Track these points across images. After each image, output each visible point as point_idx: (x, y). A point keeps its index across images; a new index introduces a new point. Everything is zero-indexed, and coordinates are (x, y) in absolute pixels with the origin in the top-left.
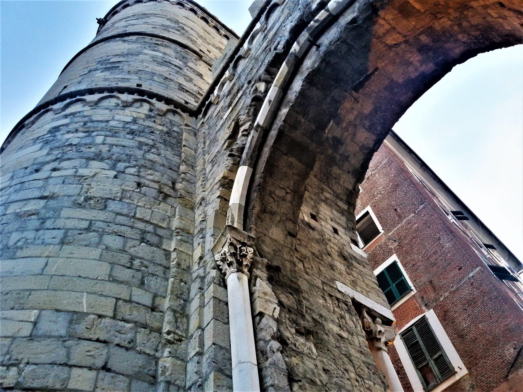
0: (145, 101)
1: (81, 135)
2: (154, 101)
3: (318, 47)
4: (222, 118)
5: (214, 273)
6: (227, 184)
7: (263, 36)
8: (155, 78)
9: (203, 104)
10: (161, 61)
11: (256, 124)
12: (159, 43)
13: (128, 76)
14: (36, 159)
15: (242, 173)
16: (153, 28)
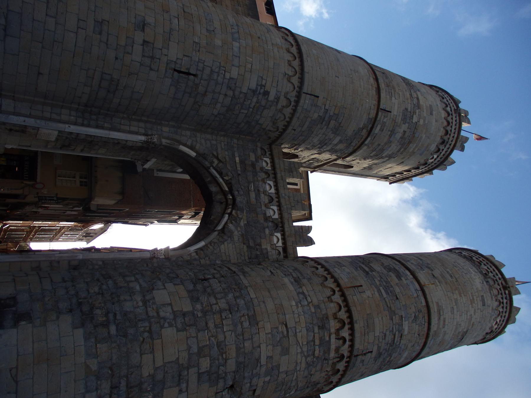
0: (278, 130)
1: (253, 104)
2: (277, 133)
3: (221, 203)
4: (239, 156)
5: (150, 133)
6: (192, 148)
7: (261, 190)
8: (303, 137)
9: (271, 150)
10: (326, 141)
11: (211, 168)
12: (353, 144)
13: (305, 127)
14: (241, 88)
15: (193, 154)
16: (379, 145)
